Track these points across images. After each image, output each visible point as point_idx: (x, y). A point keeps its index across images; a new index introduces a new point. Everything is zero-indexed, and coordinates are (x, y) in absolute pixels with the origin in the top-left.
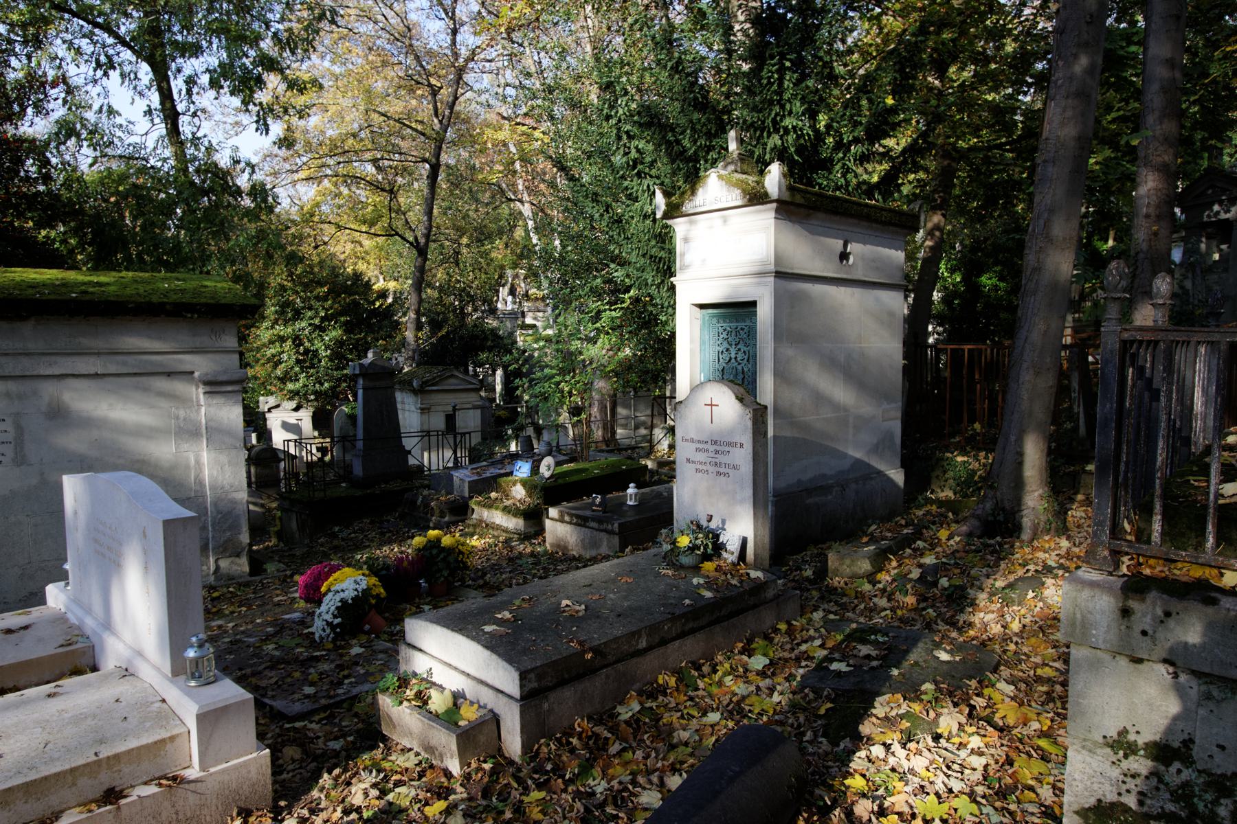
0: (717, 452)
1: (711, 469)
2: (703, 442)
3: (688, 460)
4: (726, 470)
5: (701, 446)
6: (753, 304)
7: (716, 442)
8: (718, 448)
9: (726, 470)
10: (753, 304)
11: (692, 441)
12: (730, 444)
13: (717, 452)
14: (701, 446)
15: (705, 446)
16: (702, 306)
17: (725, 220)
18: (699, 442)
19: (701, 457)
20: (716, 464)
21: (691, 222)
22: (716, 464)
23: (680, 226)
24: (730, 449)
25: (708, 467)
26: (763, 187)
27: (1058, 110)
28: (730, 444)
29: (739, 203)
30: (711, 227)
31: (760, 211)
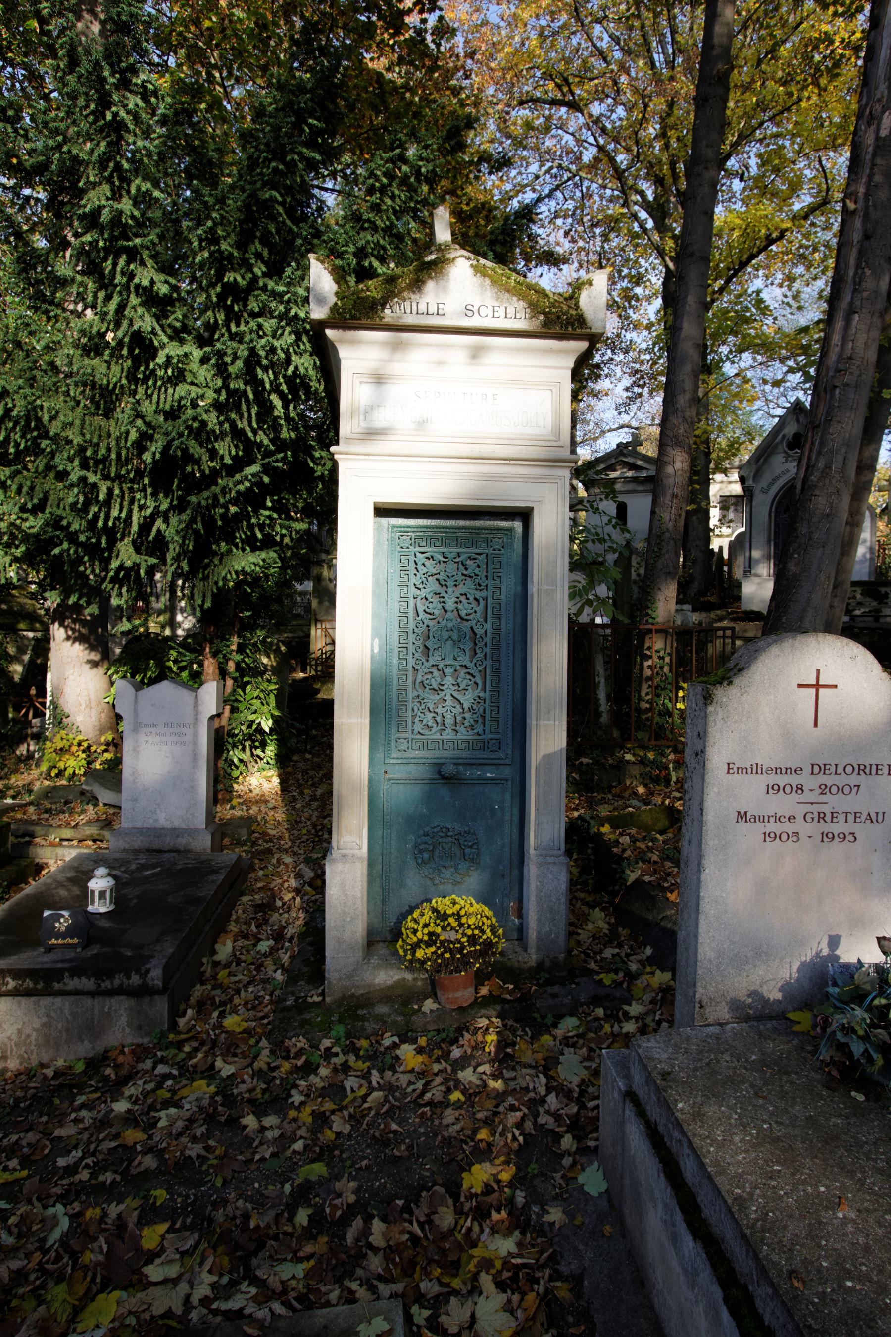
0: (824, 789)
1: (804, 828)
2: (788, 770)
3: (742, 816)
4: (851, 827)
5: (782, 780)
6: (525, 515)
7: (823, 769)
8: (828, 780)
9: (851, 827)
10: (525, 515)
11: (757, 769)
12: (861, 769)
13: (824, 789)
14: (782, 780)
15: (795, 780)
16: (382, 511)
17: (476, 353)
18: (777, 770)
19: (785, 804)
20: (821, 817)
21: (397, 346)
22: (821, 817)
23: (359, 356)
24: (862, 779)
25: (800, 826)
26: (577, 307)
27: (863, 326)
28: (861, 769)
29: (521, 325)
30: (440, 363)
31: (551, 351)
